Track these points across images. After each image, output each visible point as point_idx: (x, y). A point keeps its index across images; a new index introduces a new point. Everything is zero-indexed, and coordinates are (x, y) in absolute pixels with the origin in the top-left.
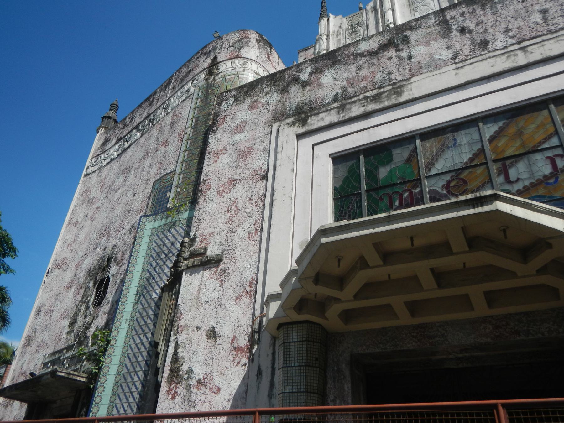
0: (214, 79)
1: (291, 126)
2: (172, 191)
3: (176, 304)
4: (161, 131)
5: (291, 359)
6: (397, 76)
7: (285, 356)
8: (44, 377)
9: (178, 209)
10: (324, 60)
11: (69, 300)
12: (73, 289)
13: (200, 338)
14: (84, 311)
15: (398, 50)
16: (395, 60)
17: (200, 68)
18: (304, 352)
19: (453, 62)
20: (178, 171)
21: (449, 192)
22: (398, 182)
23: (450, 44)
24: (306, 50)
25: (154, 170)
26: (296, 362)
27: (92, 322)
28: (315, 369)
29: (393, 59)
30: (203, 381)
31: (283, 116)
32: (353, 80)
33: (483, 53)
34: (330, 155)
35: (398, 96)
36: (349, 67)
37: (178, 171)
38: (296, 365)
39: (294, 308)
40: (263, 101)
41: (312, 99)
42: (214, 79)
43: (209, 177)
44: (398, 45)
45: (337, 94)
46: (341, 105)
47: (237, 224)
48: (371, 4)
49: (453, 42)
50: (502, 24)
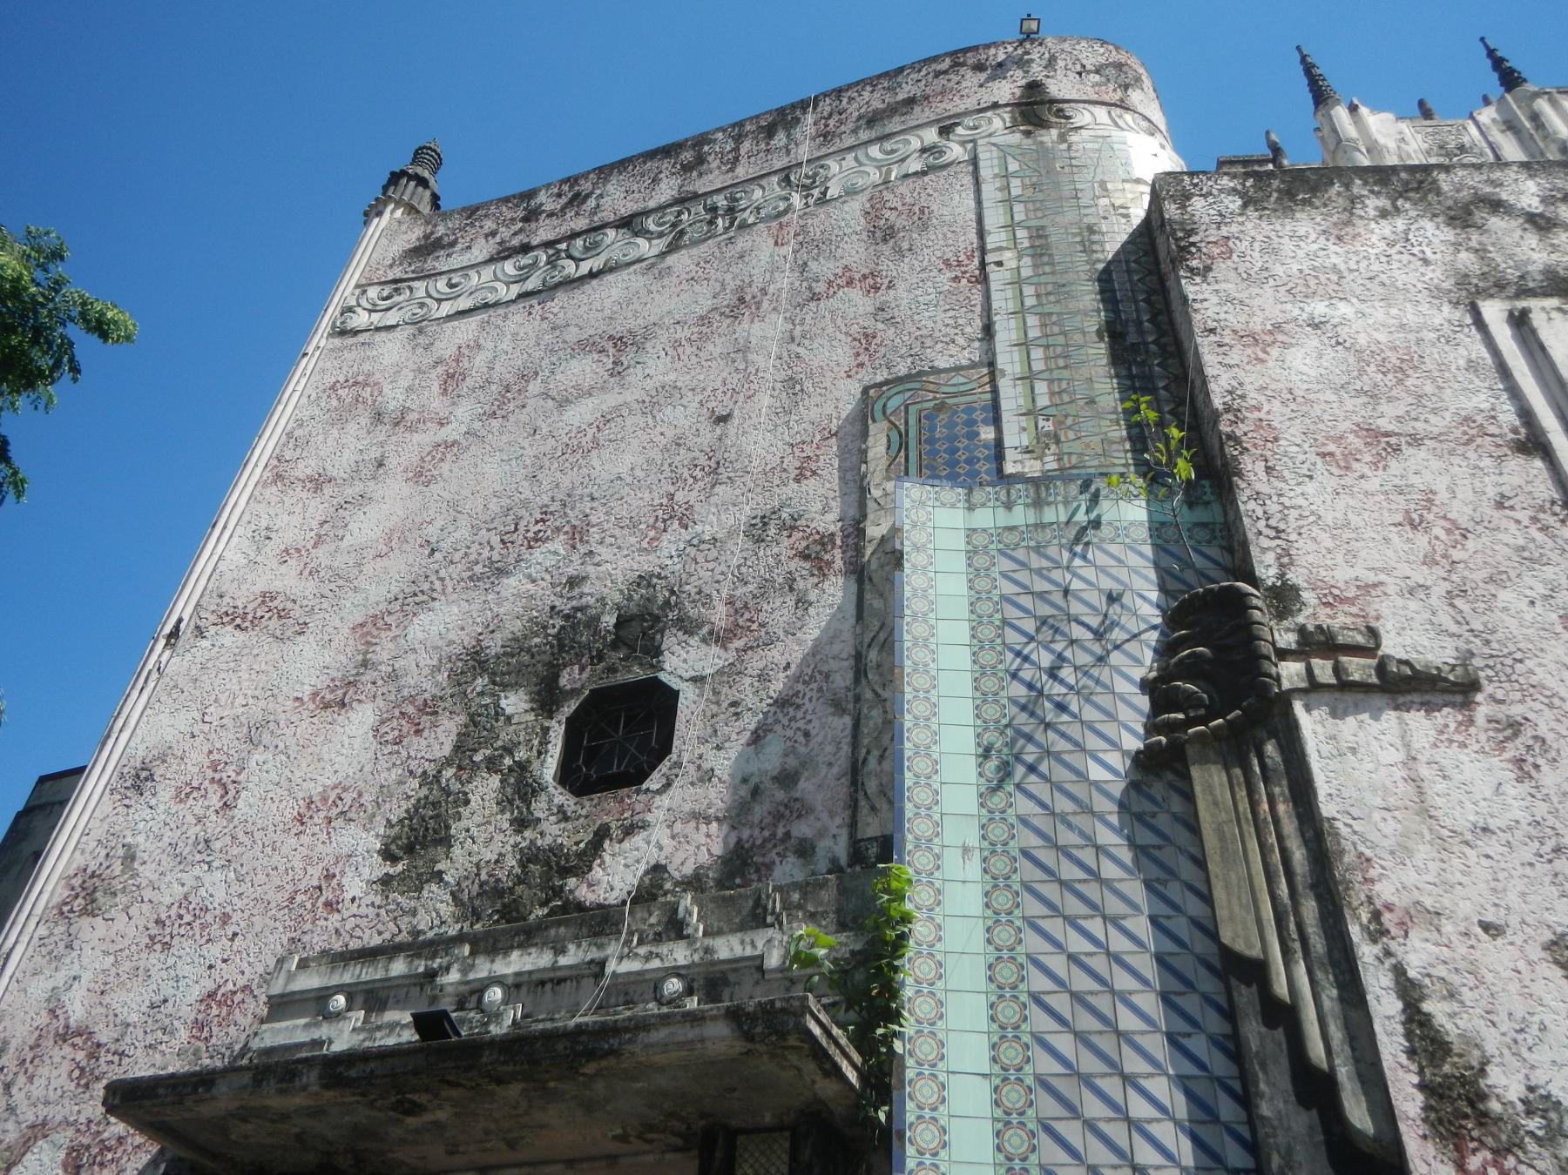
14: (504, 803)
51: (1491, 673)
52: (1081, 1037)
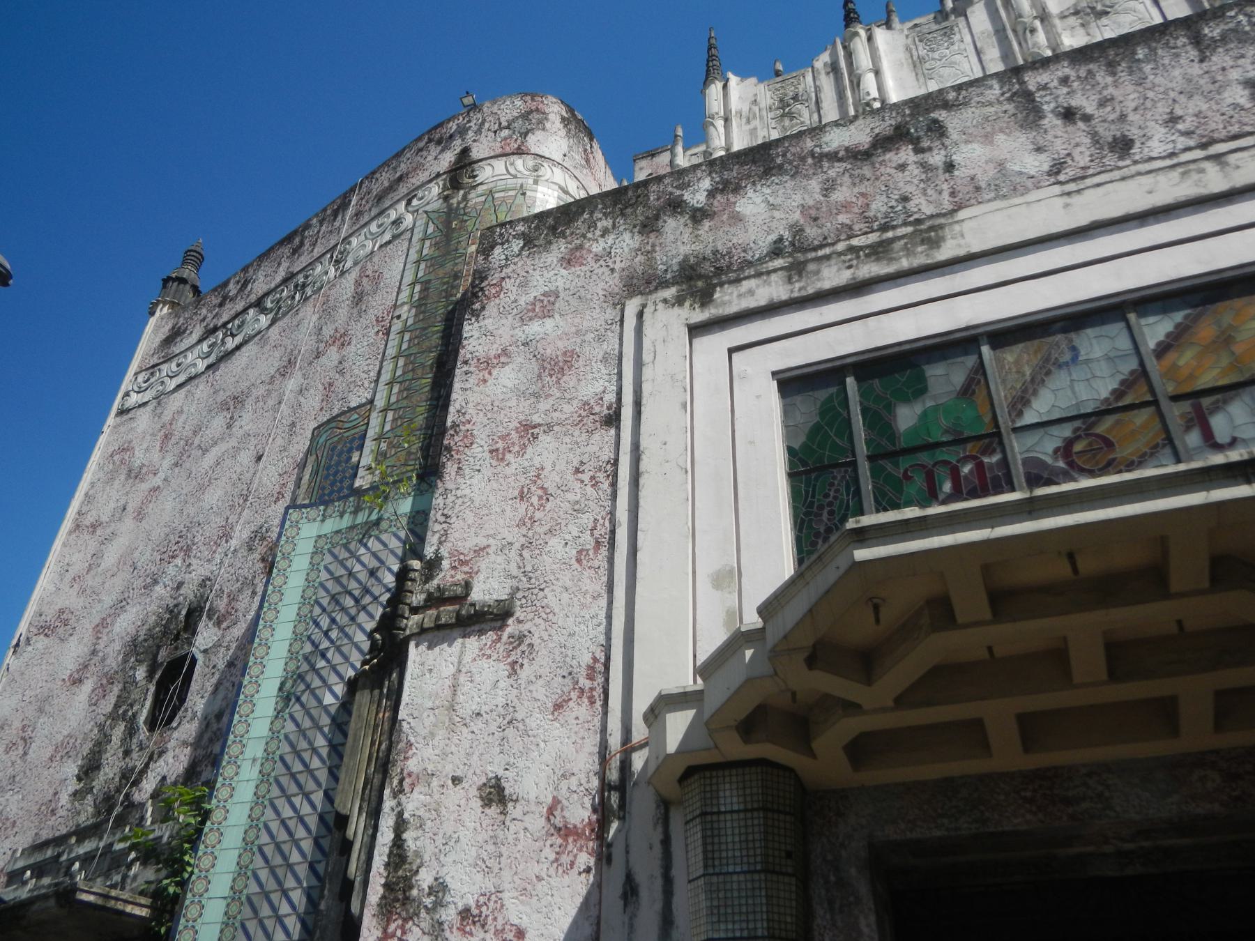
0: (465, 198)
1: (673, 305)
2: (366, 450)
3: (394, 719)
4: (328, 311)
5: (724, 854)
6: (923, 206)
7: (709, 848)
8: (36, 907)
9: (380, 492)
10: (742, 164)
11: (78, 713)
12: (88, 686)
13: (462, 807)
14: (123, 741)
15: (918, 150)
16: (914, 170)
17: (427, 173)
18: (757, 836)
19: (1052, 180)
20: (380, 403)
21: (1071, 464)
22: (944, 439)
23: (1041, 142)
24: (653, 155)
25: (312, 401)
26: (738, 861)
27: (147, 766)
28: (787, 879)
29: (909, 168)
30: (475, 911)
31: (648, 282)
32: (818, 209)
33: (1121, 164)
34: (774, 374)
35: (931, 248)
36: (805, 182)
37: (380, 403)
38: (738, 869)
39: (737, 728)
40: (597, 248)
41: (720, 248)
42: (465, 198)
43: (467, 417)
44: (918, 138)
45: (780, 239)
46: (792, 264)
47: (547, 527)
48: (825, 57)
49: (1049, 137)
50: (1159, 105)
51: (524, 601)
52: (272, 871)
